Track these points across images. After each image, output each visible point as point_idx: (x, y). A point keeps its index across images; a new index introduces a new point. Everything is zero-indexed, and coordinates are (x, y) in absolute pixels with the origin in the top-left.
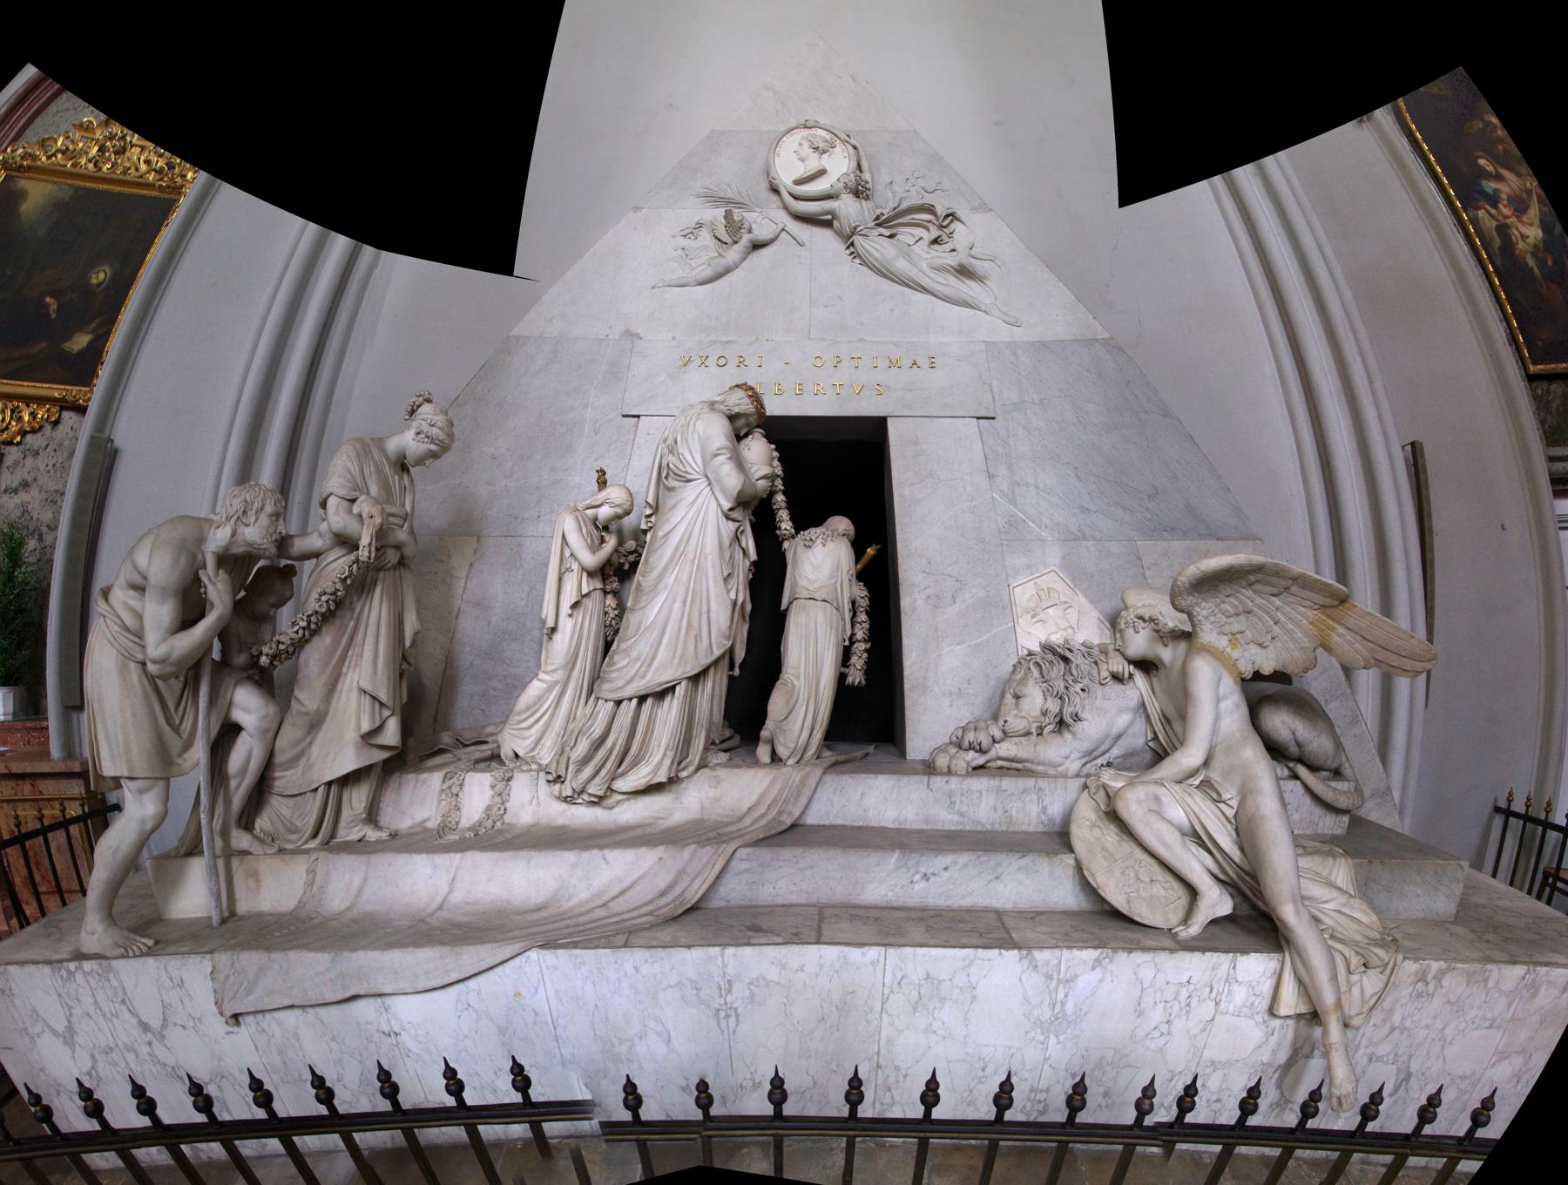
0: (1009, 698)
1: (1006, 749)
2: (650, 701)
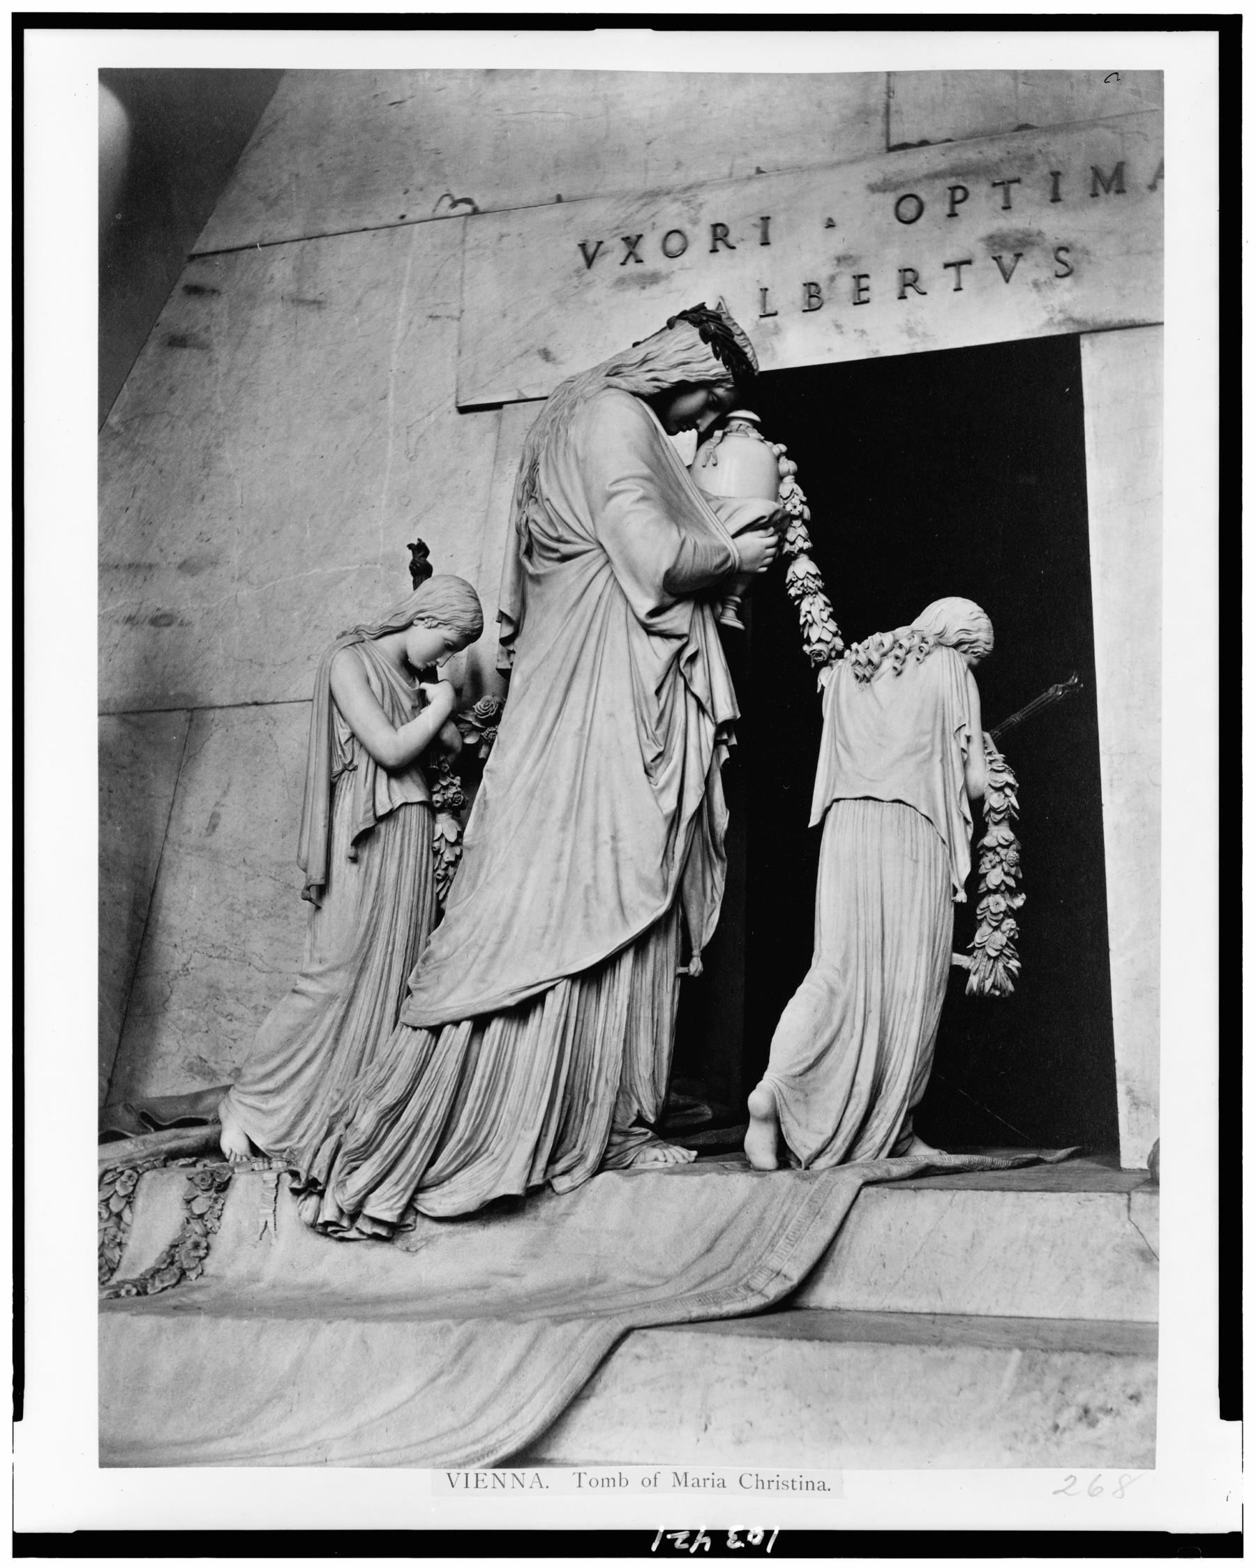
2: (497, 1026)
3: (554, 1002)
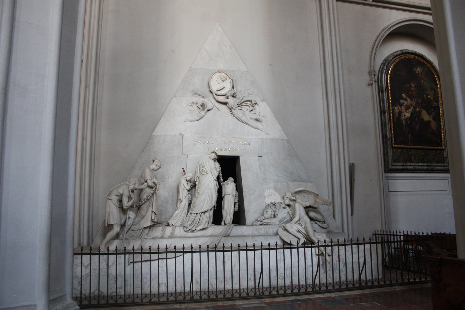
0: (265, 212)
1: (265, 221)
3: (209, 212)
